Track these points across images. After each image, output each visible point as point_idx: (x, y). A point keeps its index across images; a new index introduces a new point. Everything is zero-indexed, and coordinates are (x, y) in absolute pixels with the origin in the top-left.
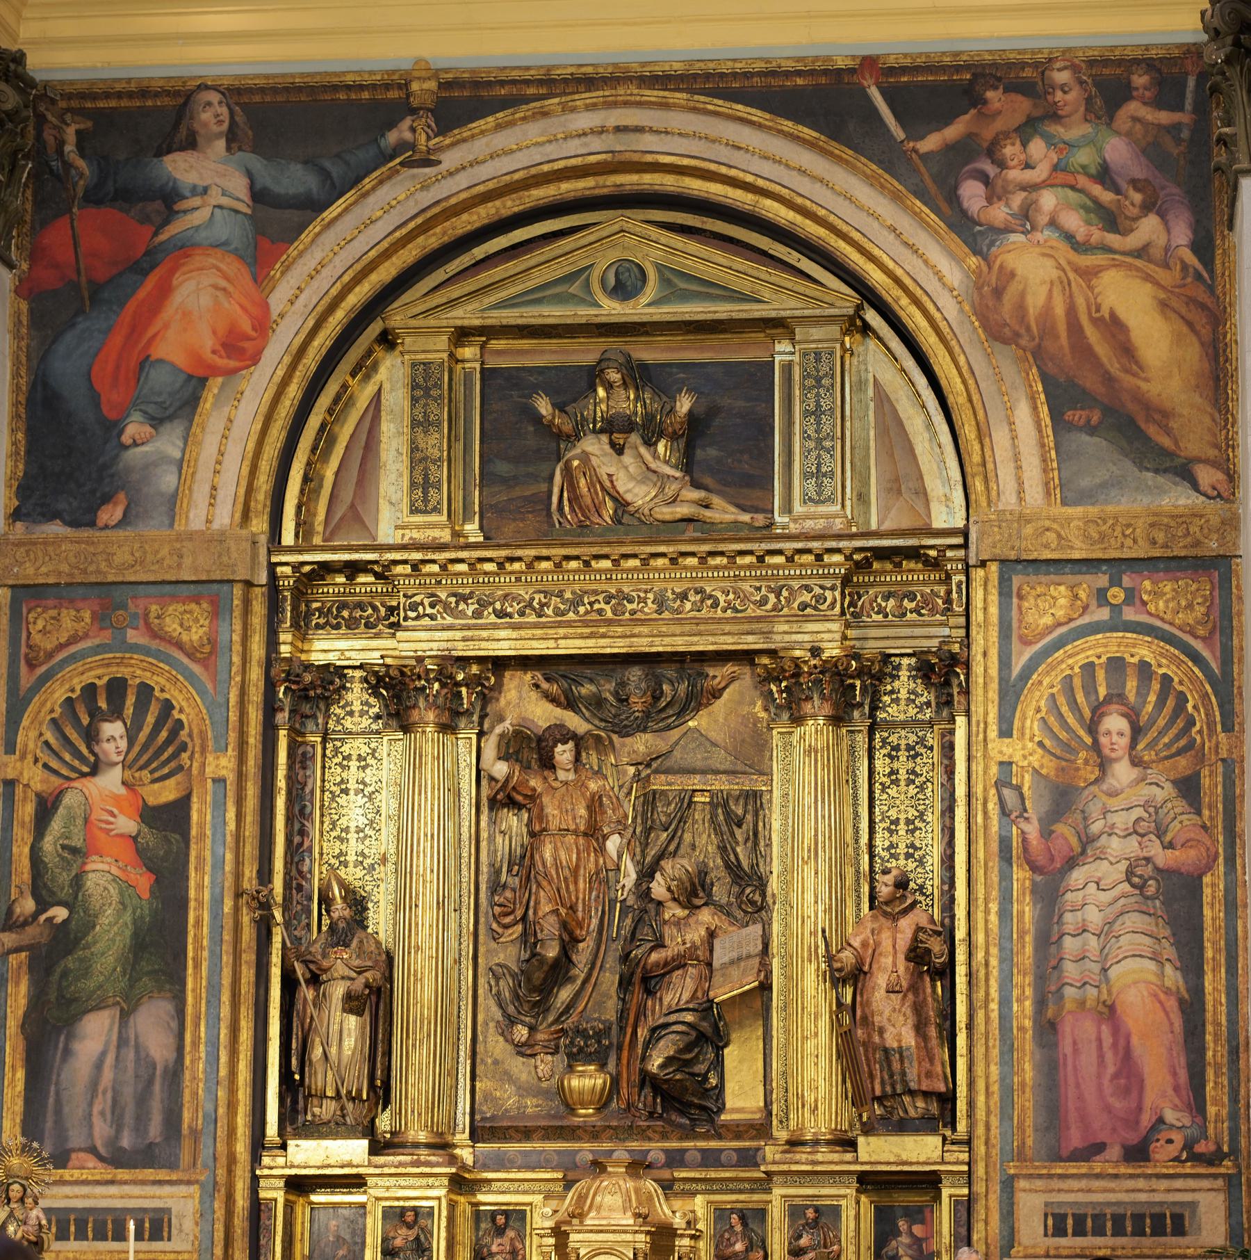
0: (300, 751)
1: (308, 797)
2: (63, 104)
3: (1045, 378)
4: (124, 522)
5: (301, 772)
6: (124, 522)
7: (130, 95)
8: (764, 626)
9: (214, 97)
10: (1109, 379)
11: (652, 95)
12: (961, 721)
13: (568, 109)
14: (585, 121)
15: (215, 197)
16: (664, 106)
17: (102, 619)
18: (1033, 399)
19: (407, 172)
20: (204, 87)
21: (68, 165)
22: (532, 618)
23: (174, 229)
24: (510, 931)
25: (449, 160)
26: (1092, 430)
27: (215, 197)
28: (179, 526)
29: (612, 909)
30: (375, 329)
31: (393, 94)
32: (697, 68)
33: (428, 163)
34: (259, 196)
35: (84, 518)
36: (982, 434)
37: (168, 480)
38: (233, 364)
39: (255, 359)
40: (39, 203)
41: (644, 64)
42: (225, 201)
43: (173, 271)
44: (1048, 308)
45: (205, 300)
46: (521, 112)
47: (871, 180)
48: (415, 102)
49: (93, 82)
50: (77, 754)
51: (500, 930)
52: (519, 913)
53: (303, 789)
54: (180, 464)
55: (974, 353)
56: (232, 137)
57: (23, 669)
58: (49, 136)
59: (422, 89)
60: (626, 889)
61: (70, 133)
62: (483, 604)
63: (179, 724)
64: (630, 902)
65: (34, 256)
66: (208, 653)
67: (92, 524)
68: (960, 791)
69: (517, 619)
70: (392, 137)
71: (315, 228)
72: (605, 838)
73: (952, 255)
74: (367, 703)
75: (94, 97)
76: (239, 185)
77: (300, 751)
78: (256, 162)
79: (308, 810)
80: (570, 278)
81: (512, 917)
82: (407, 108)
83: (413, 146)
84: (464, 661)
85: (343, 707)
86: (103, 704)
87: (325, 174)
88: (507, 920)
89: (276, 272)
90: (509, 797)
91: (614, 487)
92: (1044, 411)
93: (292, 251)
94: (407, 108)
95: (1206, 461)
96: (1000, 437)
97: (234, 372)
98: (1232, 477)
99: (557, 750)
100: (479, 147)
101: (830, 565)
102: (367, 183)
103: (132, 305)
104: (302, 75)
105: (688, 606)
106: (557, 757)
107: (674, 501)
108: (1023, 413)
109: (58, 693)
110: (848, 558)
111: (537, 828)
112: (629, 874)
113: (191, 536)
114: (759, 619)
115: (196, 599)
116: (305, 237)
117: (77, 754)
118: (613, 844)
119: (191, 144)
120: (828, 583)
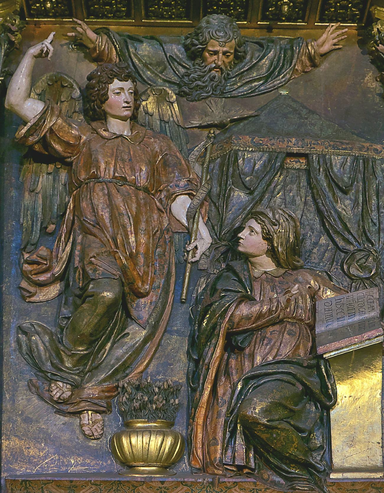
24: (45, 290)
29: (180, 274)
51: (32, 289)
52: (58, 269)
64: (204, 264)
72: (171, 197)
81: (49, 275)
88: (42, 278)
99: (112, 86)
106: (112, 96)
111: (83, 176)
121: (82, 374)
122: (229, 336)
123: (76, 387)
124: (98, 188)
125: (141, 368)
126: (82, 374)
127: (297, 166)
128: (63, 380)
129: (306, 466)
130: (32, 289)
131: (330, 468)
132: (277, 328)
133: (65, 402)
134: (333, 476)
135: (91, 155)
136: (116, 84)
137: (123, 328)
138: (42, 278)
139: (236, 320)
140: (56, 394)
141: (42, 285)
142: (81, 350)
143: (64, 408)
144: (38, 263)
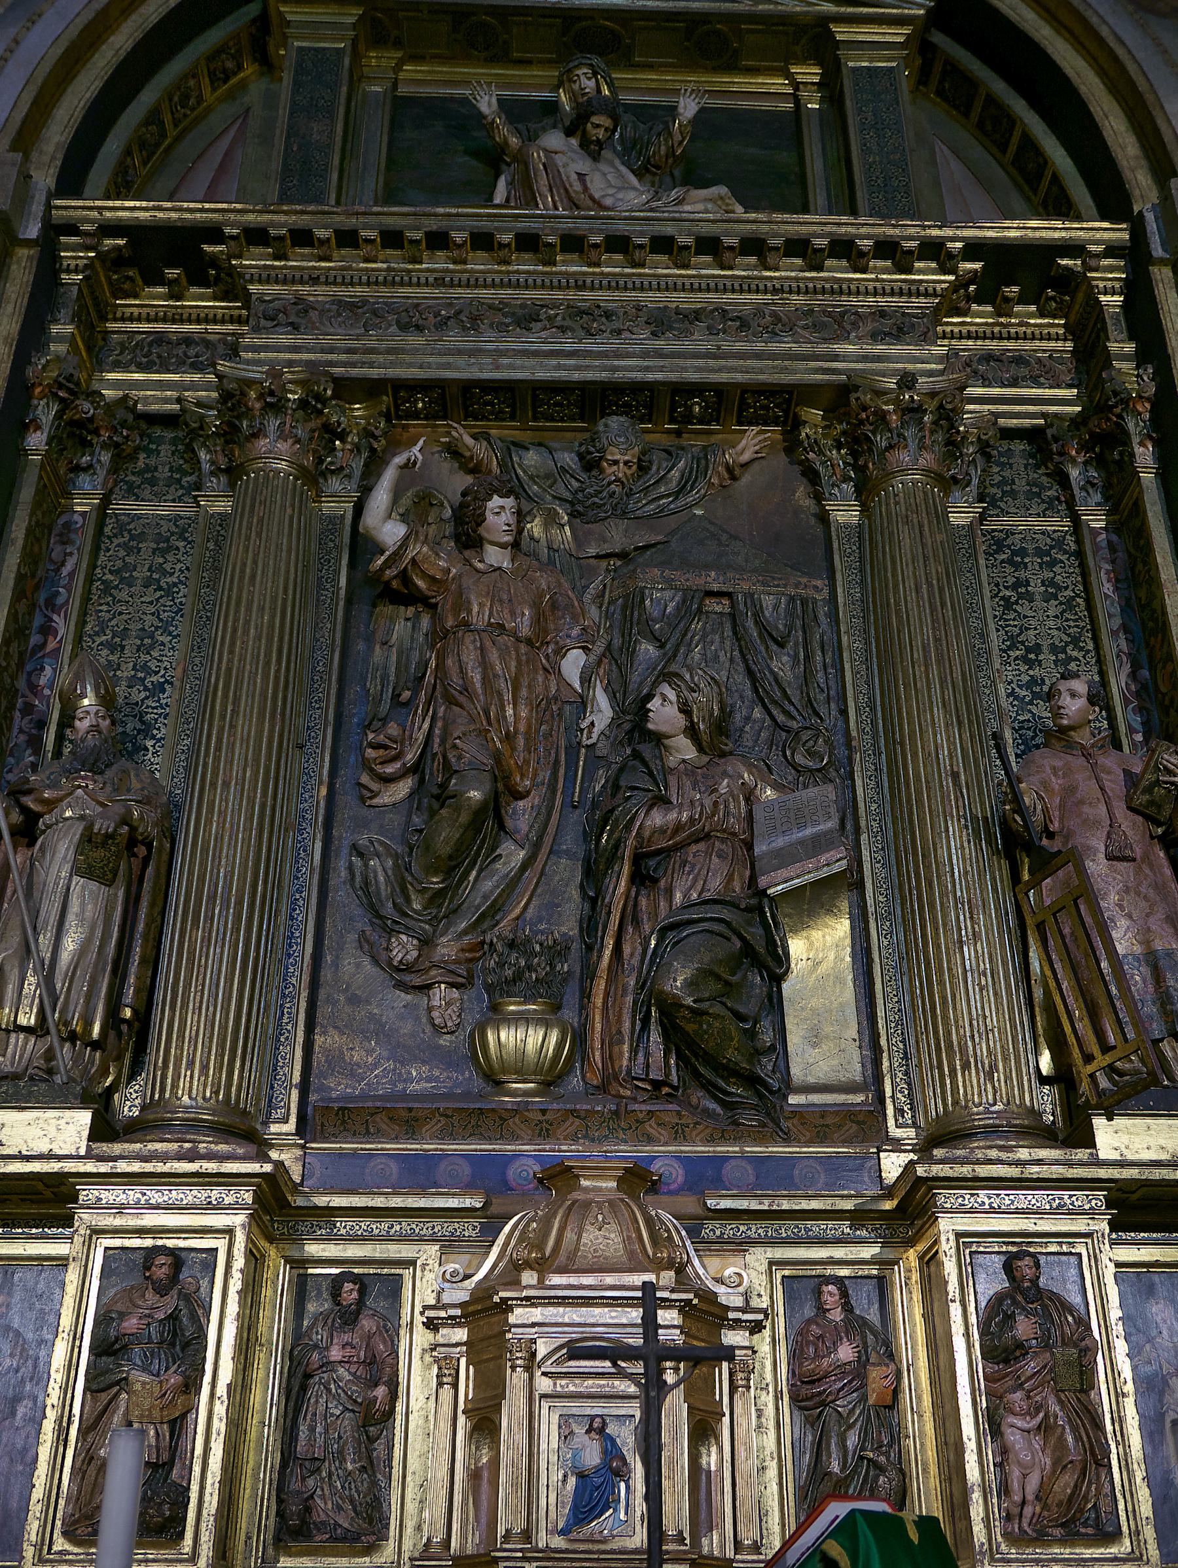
0: (61, 521)
1: (64, 582)
5: (58, 549)
24: (393, 787)
51: (375, 786)
52: (410, 757)
53: (58, 570)
60: (596, 731)
64: (602, 750)
72: (561, 652)
74: (180, 470)
77: (61, 521)
79: (60, 600)
81: (398, 765)
84: (346, 389)
85: (140, 473)
88: (389, 769)
90: (404, 576)
91: (586, 189)
99: (490, 504)
106: (490, 517)
111: (450, 623)
112: (602, 712)
118: (573, 664)
121: (434, 921)
122: (638, 859)
123: (426, 943)
124: (468, 638)
125: (517, 911)
126: (434, 921)
127: (718, 609)
128: (408, 931)
129: (753, 1081)
130: (375, 786)
131: (788, 1086)
132: (702, 846)
133: (409, 968)
134: (793, 1100)
135: (461, 594)
136: (496, 501)
137: (494, 848)
138: (389, 769)
139: (647, 834)
140: (397, 955)
141: (388, 780)
142: (436, 882)
143: (407, 978)
144: (386, 747)
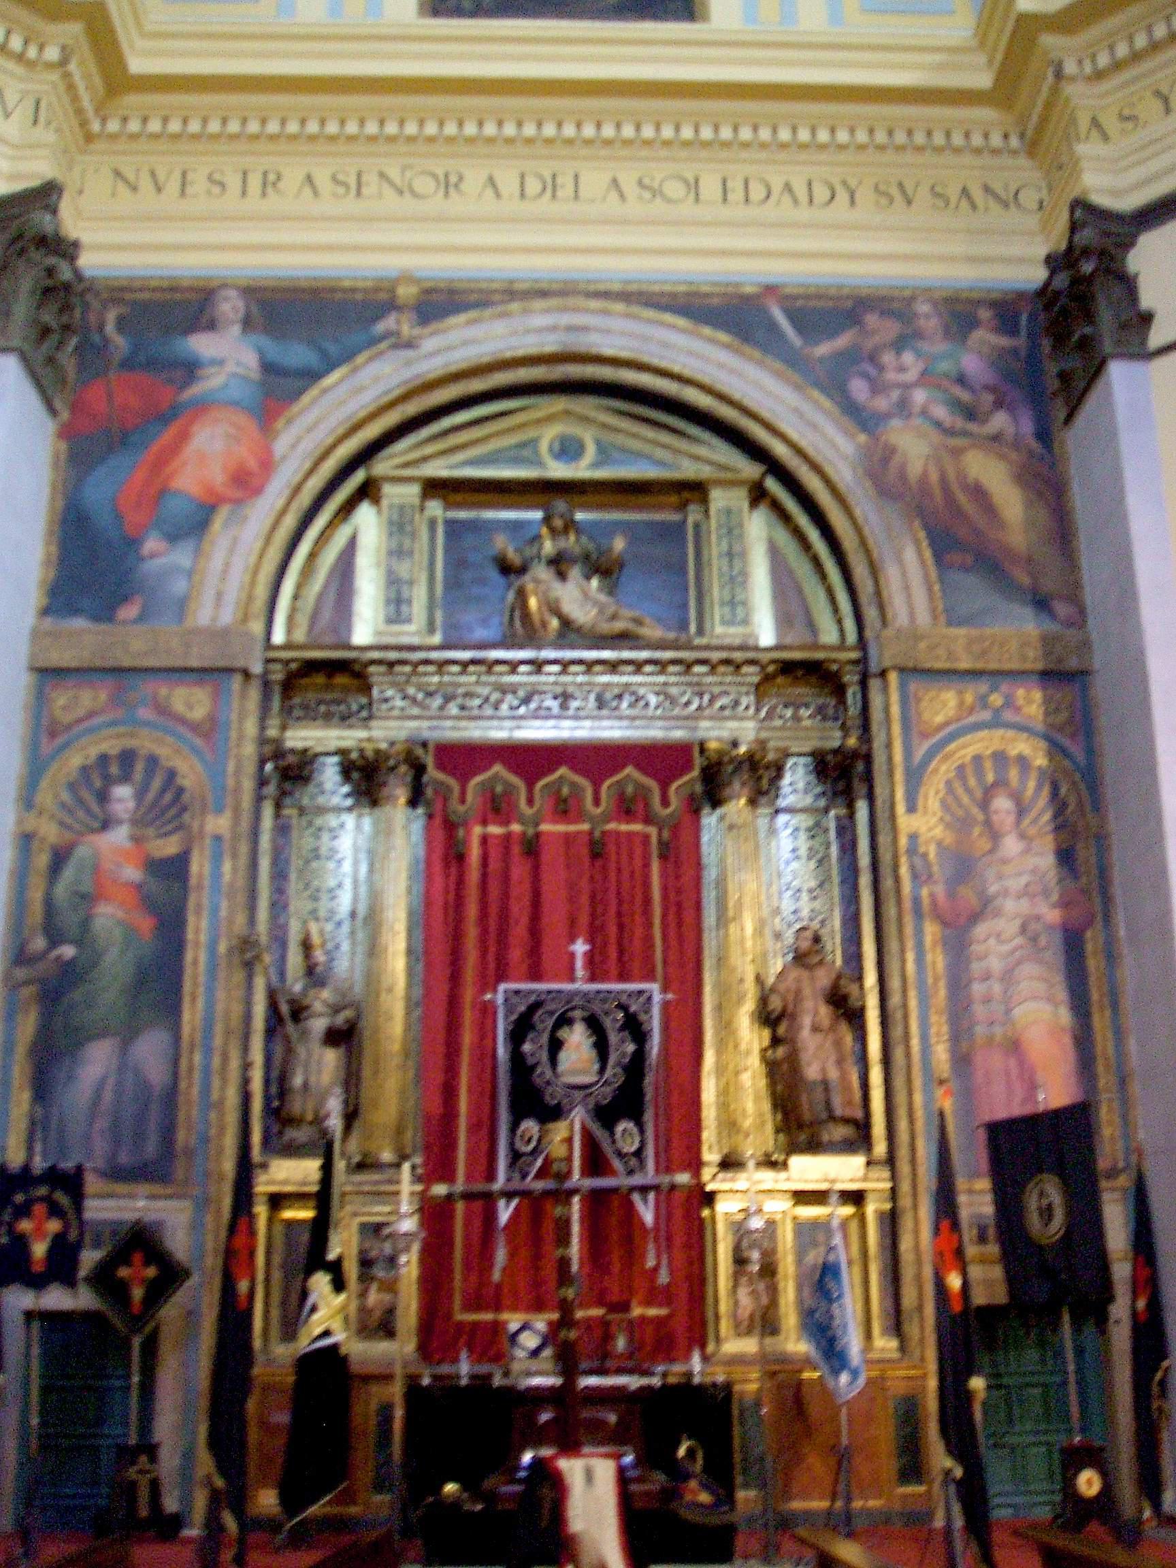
2: (105, 296)
3: (926, 527)
4: (142, 618)
6: (142, 618)
7: (163, 290)
8: (690, 723)
9: (233, 293)
10: (977, 532)
11: (594, 304)
12: (862, 808)
13: (526, 312)
14: (539, 321)
15: (231, 367)
16: (605, 312)
17: (116, 700)
18: (917, 543)
19: (392, 355)
20: (224, 286)
21: (106, 341)
22: (488, 711)
23: (196, 390)
25: (429, 345)
26: (966, 569)
27: (231, 367)
28: (189, 623)
30: (359, 476)
31: (383, 296)
32: (633, 287)
33: (410, 345)
34: (269, 368)
35: (105, 613)
36: (874, 570)
37: (179, 586)
38: (238, 494)
39: (257, 491)
40: (81, 367)
41: (589, 281)
42: (240, 370)
43: (191, 422)
44: (925, 474)
45: (218, 446)
46: (488, 312)
47: (778, 374)
48: (400, 302)
49: (132, 279)
50: (88, 811)
54: (190, 574)
55: (865, 506)
56: (247, 324)
57: (44, 739)
58: (92, 318)
59: (406, 292)
61: (111, 316)
62: (448, 699)
63: (181, 791)
65: (75, 407)
66: (210, 729)
67: (110, 619)
68: (864, 860)
69: (476, 712)
70: (380, 327)
71: (313, 392)
73: (846, 433)
75: (129, 289)
76: (250, 360)
78: (265, 341)
80: (523, 445)
82: (391, 305)
83: (398, 334)
86: (114, 770)
87: (324, 354)
89: (280, 424)
92: (928, 554)
93: (295, 408)
94: (391, 305)
95: (1060, 597)
96: (891, 574)
97: (238, 502)
98: (1082, 611)
100: (454, 337)
101: (746, 675)
102: (360, 359)
103: (155, 448)
104: (307, 279)
105: (625, 704)
107: (614, 617)
108: (910, 554)
109: (76, 760)
110: (763, 667)
113: (197, 631)
114: (687, 718)
115: (200, 683)
116: (306, 399)
117: (88, 811)
119: (212, 326)
120: (744, 689)
